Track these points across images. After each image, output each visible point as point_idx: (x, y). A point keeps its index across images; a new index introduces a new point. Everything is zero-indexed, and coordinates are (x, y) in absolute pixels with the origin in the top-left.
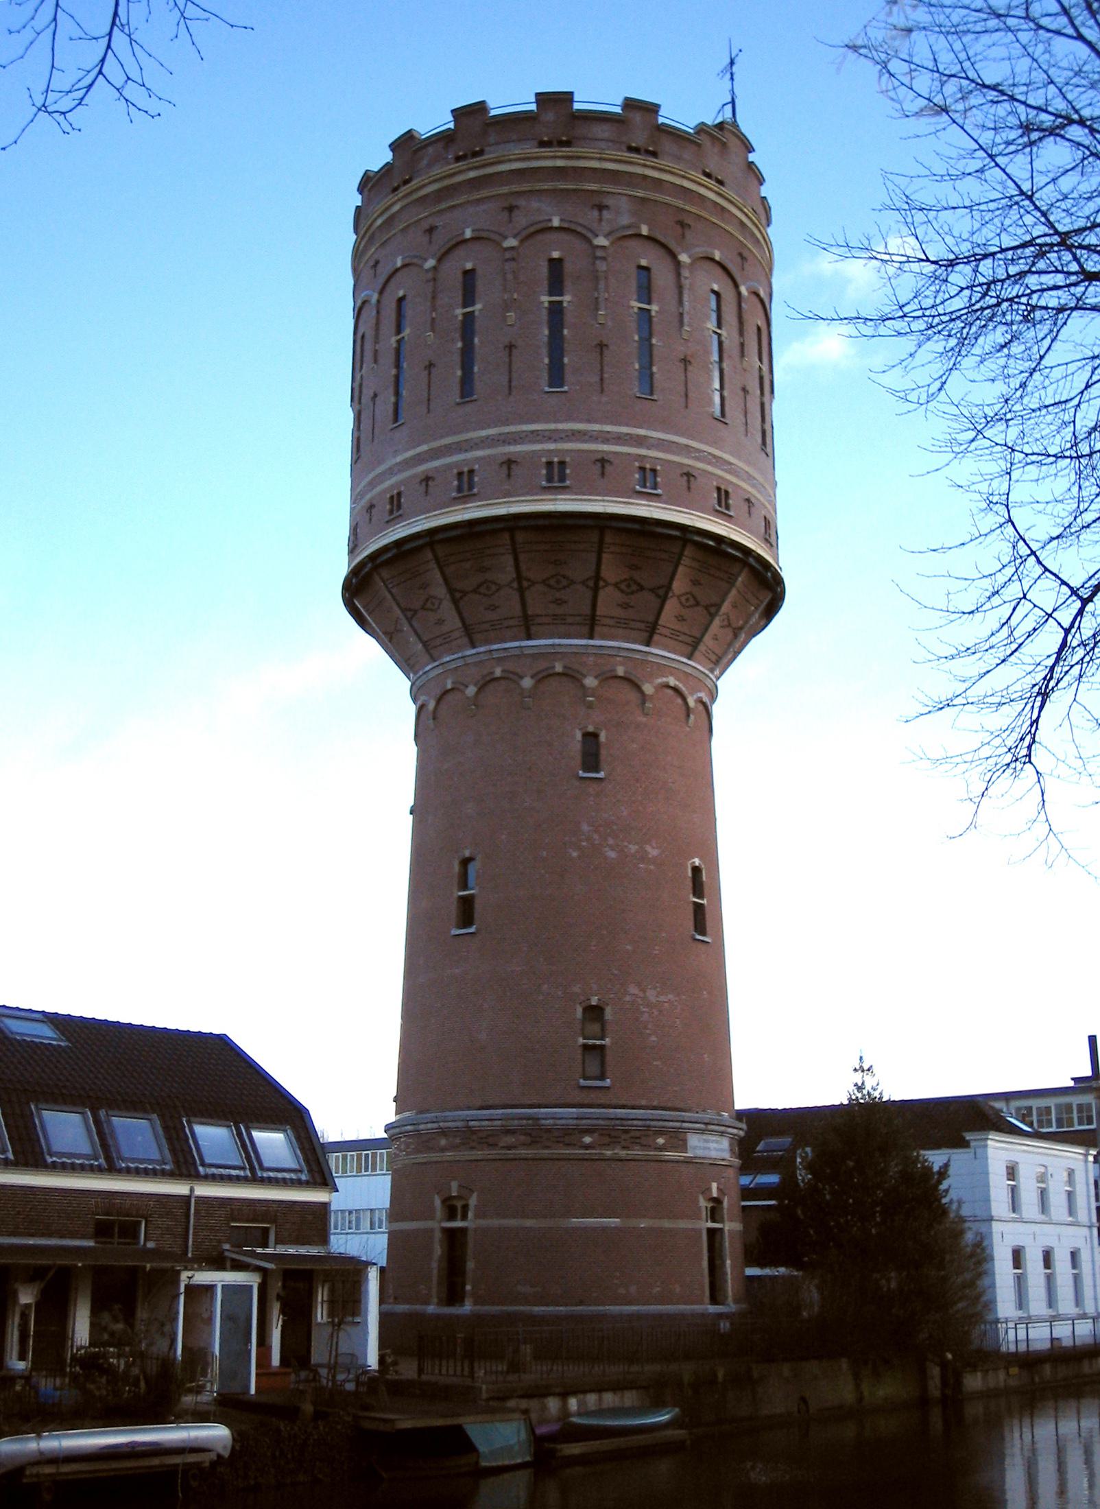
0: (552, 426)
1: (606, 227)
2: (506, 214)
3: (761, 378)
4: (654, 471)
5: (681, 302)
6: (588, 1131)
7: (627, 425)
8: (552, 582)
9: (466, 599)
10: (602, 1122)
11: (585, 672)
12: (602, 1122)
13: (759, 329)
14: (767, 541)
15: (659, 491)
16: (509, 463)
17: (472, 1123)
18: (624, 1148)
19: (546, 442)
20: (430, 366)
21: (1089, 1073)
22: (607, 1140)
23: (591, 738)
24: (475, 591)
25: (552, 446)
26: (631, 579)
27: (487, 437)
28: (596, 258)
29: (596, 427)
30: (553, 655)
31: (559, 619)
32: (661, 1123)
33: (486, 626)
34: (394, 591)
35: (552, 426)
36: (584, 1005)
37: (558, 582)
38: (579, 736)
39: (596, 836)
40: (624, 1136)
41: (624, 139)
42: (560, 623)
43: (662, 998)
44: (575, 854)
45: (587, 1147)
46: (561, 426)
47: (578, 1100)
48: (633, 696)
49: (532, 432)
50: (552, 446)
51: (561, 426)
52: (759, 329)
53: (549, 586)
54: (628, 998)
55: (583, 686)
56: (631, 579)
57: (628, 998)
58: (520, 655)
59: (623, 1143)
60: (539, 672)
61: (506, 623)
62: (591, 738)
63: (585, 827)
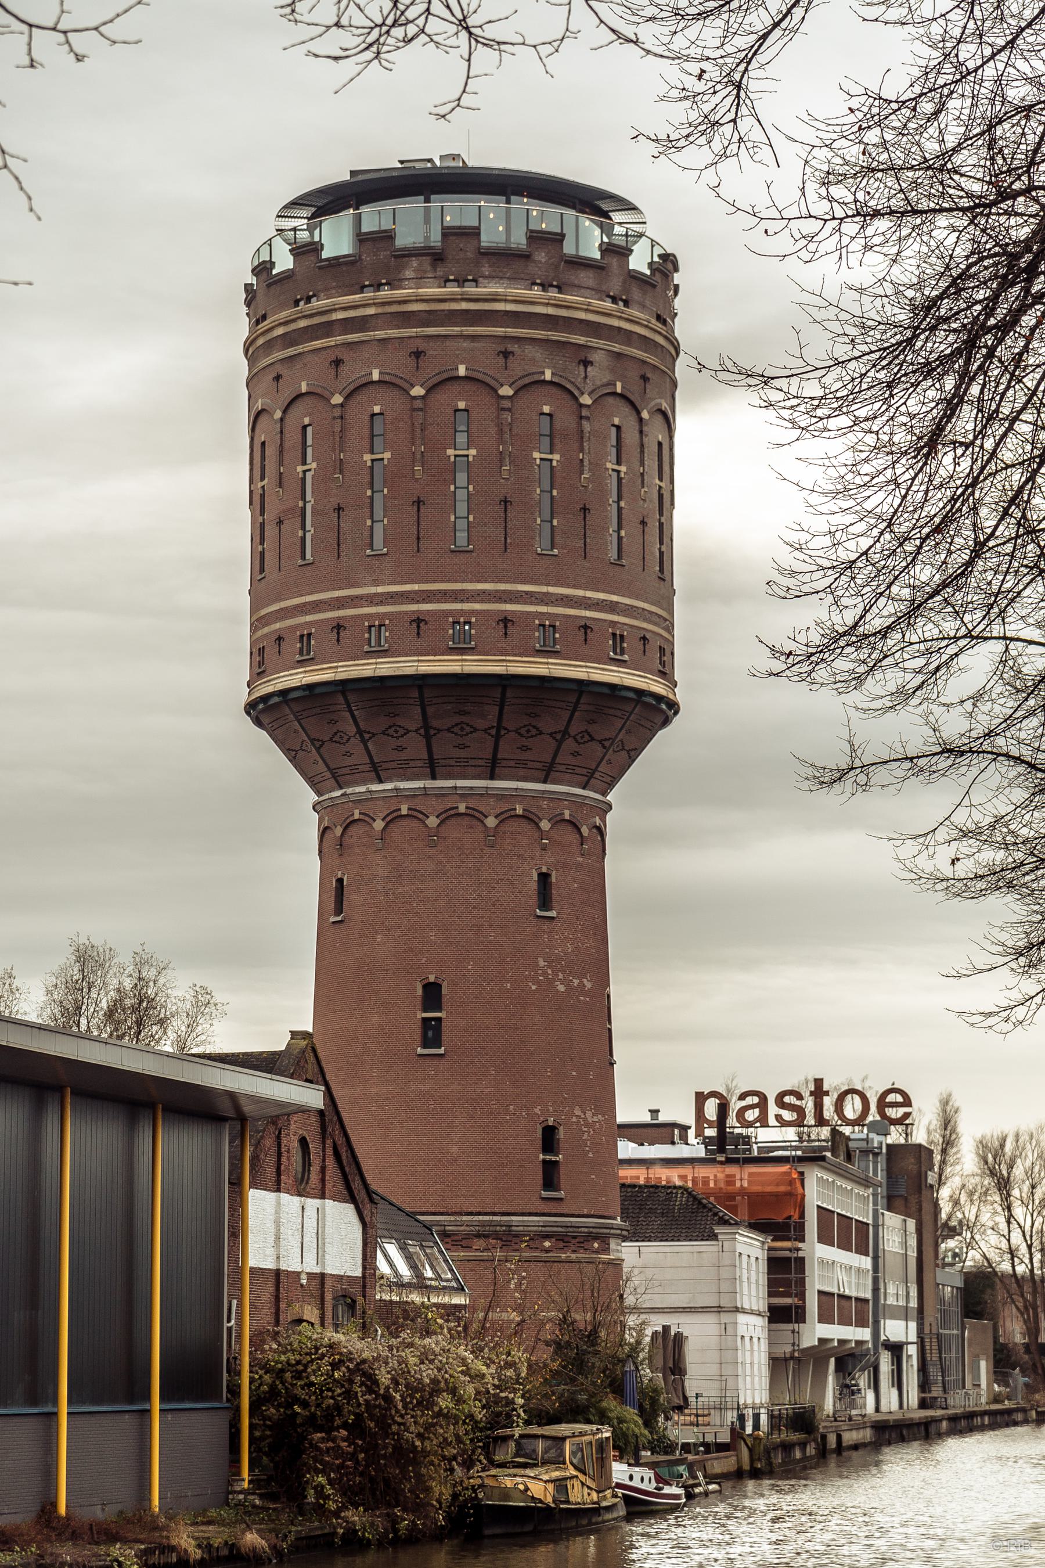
0: (544, 589)
1: (590, 386)
2: (501, 360)
3: (661, 497)
4: (622, 636)
5: (642, 464)
6: (547, 1237)
7: (603, 592)
8: (523, 731)
9: (438, 736)
10: (560, 1229)
11: (540, 815)
12: (560, 1229)
13: (660, 444)
14: (663, 674)
15: (626, 657)
16: (506, 621)
17: (447, 1228)
18: (574, 1251)
19: (538, 604)
20: (419, 502)
21: (620, 1156)
22: (561, 1244)
23: (544, 878)
24: (449, 730)
25: (543, 609)
26: (586, 731)
27: (484, 592)
28: (581, 418)
29: (580, 593)
30: (518, 795)
31: (522, 764)
32: (598, 1230)
33: (452, 762)
34: (356, 713)
35: (544, 589)
36: (543, 1125)
37: (528, 731)
38: (535, 877)
39: (550, 971)
40: (574, 1241)
41: (604, 288)
42: (523, 770)
43: (595, 1119)
44: (534, 987)
45: (547, 1251)
46: (551, 589)
47: (540, 1210)
48: (574, 838)
49: (527, 593)
50: (543, 609)
51: (551, 589)
52: (660, 444)
53: (519, 734)
54: (574, 1119)
55: (539, 828)
56: (586, 731)
57: (574, 1119)
58: (485, 794)
59: (574, 1248)
60: (502, 813)
61: (472, 762)
62: (544, 878)
63: (542, 963)
